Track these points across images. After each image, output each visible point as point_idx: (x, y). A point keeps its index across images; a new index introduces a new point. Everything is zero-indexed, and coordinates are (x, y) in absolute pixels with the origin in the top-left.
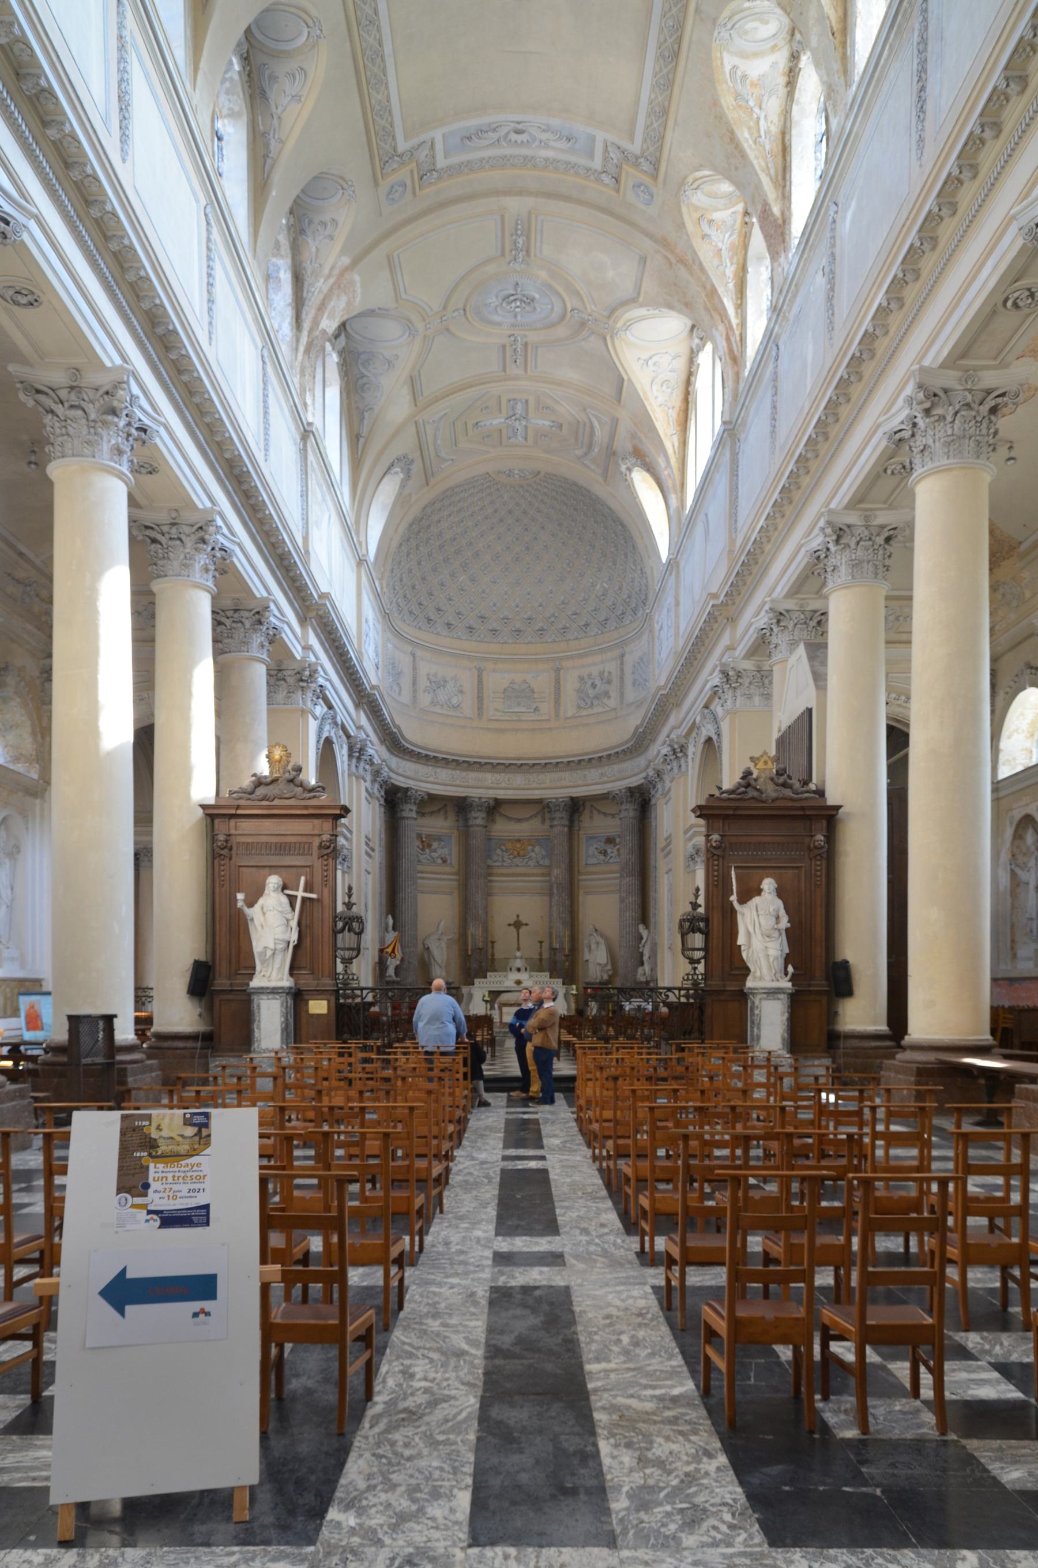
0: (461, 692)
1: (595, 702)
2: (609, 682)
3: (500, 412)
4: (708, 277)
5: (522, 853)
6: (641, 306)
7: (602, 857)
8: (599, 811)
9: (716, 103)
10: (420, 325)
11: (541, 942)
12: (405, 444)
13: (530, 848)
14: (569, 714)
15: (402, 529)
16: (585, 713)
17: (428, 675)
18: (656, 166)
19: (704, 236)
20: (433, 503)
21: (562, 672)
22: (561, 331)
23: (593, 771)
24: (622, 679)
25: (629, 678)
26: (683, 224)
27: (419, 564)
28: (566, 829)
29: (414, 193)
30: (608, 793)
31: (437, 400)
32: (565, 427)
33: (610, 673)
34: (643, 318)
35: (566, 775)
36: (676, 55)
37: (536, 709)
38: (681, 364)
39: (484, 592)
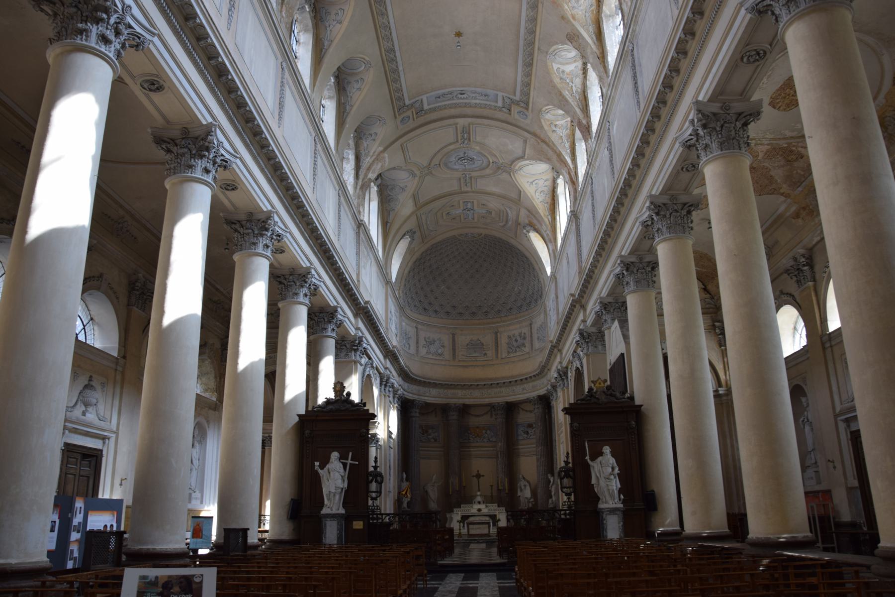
0: (443, 346)
1: (518, 350)
2: (525, 338)
3: (460, 207)
4: (557, 148)
6: (527, 160)
7: (525, 436)
8: (523, 409)
9: (552, 81)
10: (418, 173)
11: (492, 486)
12: (411, 224)
13: (484, 431)
14: (504, 356)
15: (410, 265)
16: (512, 355)
17: (425, 338)
18: (527, 104)
19: (553, 131)
20: (426, 251)
21: (498, 334)
22: (488, 171)
23: (518, 386)
24: (531, 336)
25: (535, 336)
26: (543, 126)
27: (419, 281)
28: (504, 420)
29: (414, 120)
30: (528, 399)
31: (427, 204)
32: (493, 213)
33: (525, 334)
34: (528, 165)
35: (503, 389)
36: (531, 65)
37: (485, 354)
38: (549, 183)
39: (454, 294)
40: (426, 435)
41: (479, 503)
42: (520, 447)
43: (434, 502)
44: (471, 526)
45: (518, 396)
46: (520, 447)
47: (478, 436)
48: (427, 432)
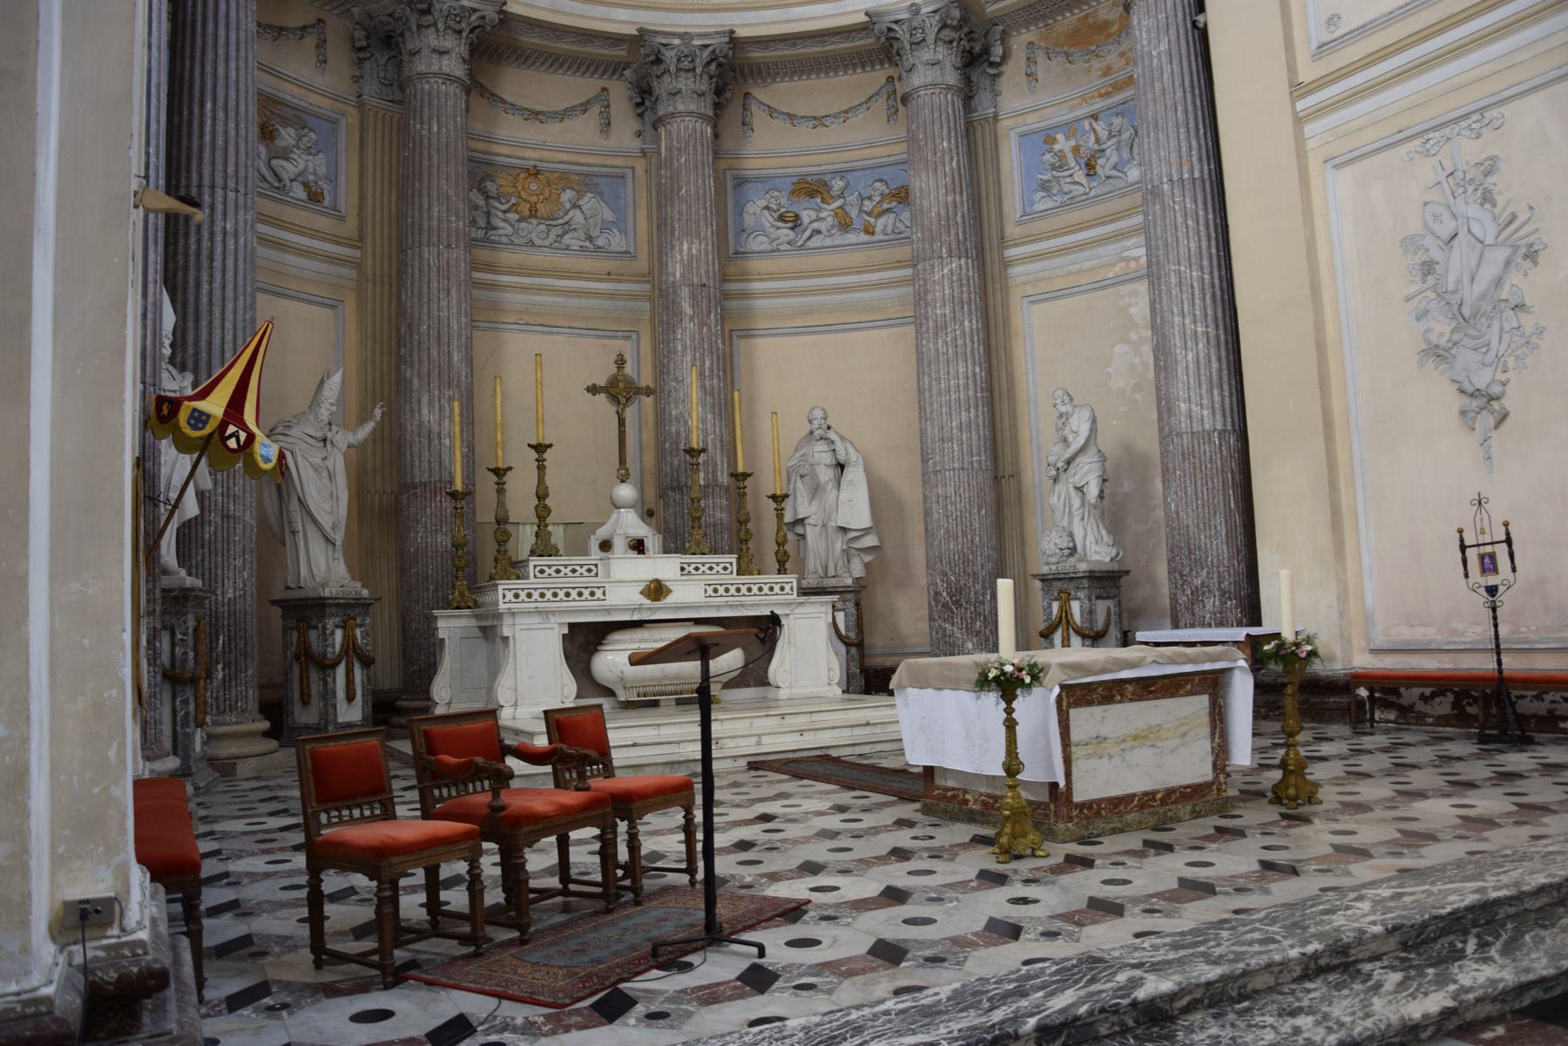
5: (543, 209)
7: (785, 233)
8: (772, 111)
41: (638, 546)
42: (757, 286)
43: (329, 541)
44: (1085, 720)
46: (757, 286)
47: (533, 213)
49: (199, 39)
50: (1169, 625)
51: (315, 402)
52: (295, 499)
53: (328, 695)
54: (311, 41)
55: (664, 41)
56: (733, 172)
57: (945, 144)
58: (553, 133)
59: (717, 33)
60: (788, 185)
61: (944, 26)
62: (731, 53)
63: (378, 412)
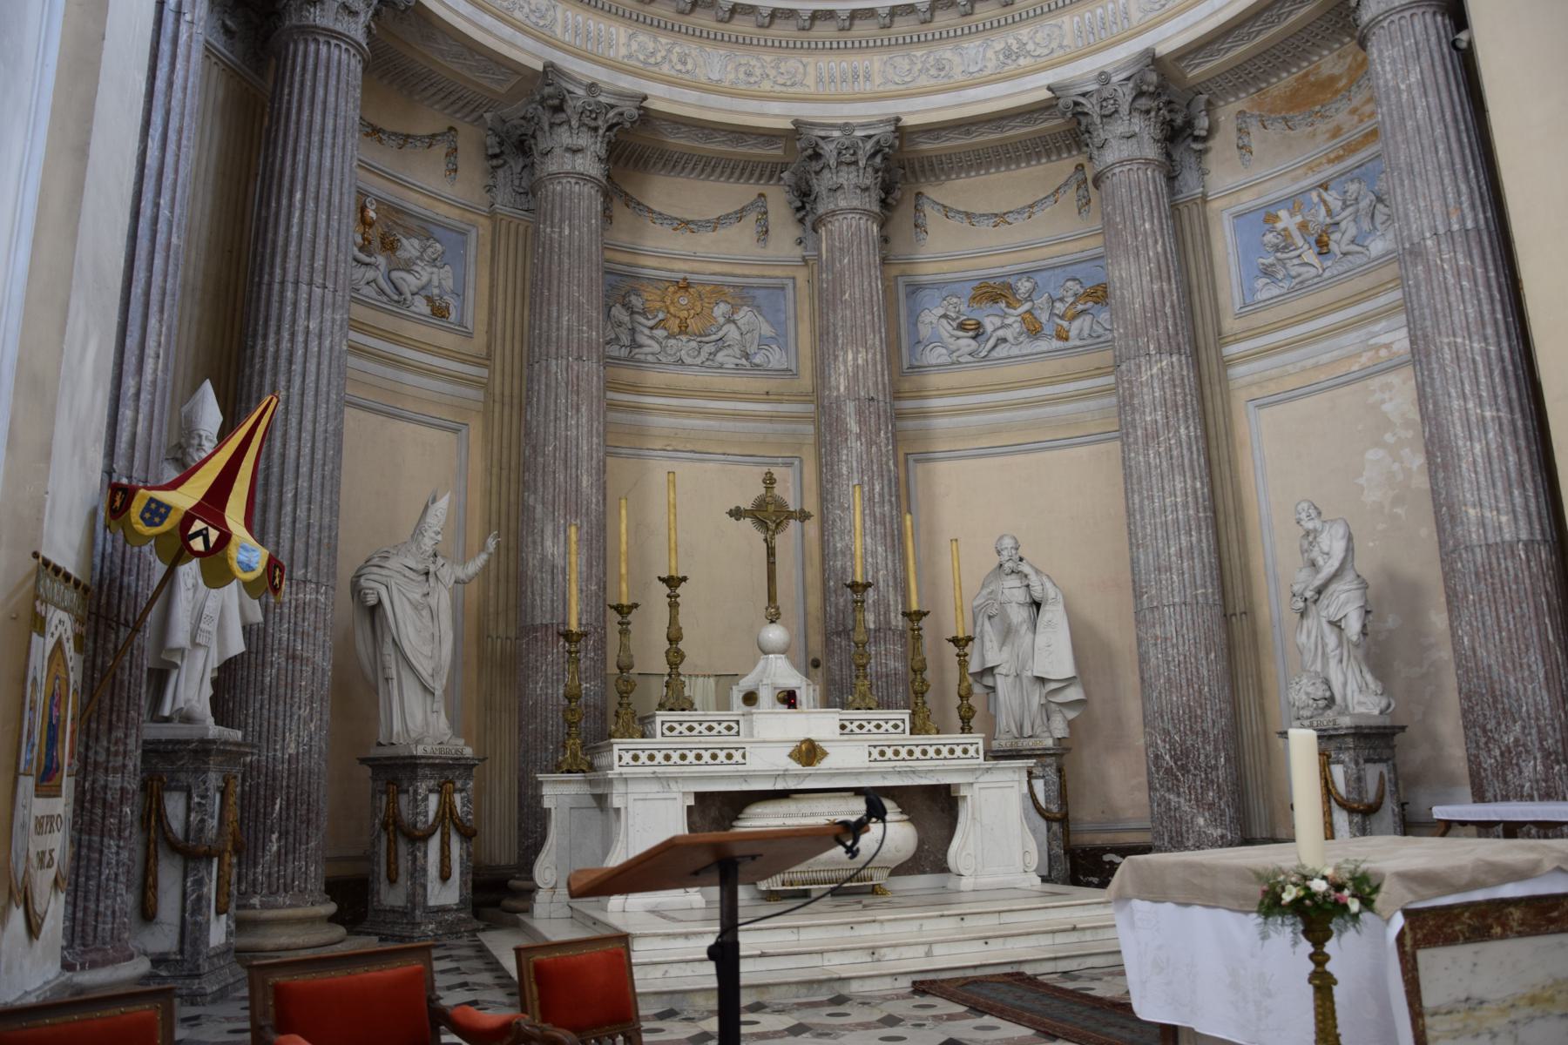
7: (966, 343)
8: (947, 211)
23: (972, 47)
40: (381, 260)
41: (789, 699)
43: (427, 690)
45: (971, 93)
47: (683, 329)
48: (389, 245)
49: (292, 126)
50: (1470, 798)
51: (418, 531)
52: (389, 640)
53: (418, 872)
54: (440, 150)
55: (823, 133)
56: (906, 279)
57: (1147, 226)
58: (705, 242)
59: (881, 122)
60: (968, 290)
61: (1140, 94)
62: (897, 143)
63: (491, 544)
